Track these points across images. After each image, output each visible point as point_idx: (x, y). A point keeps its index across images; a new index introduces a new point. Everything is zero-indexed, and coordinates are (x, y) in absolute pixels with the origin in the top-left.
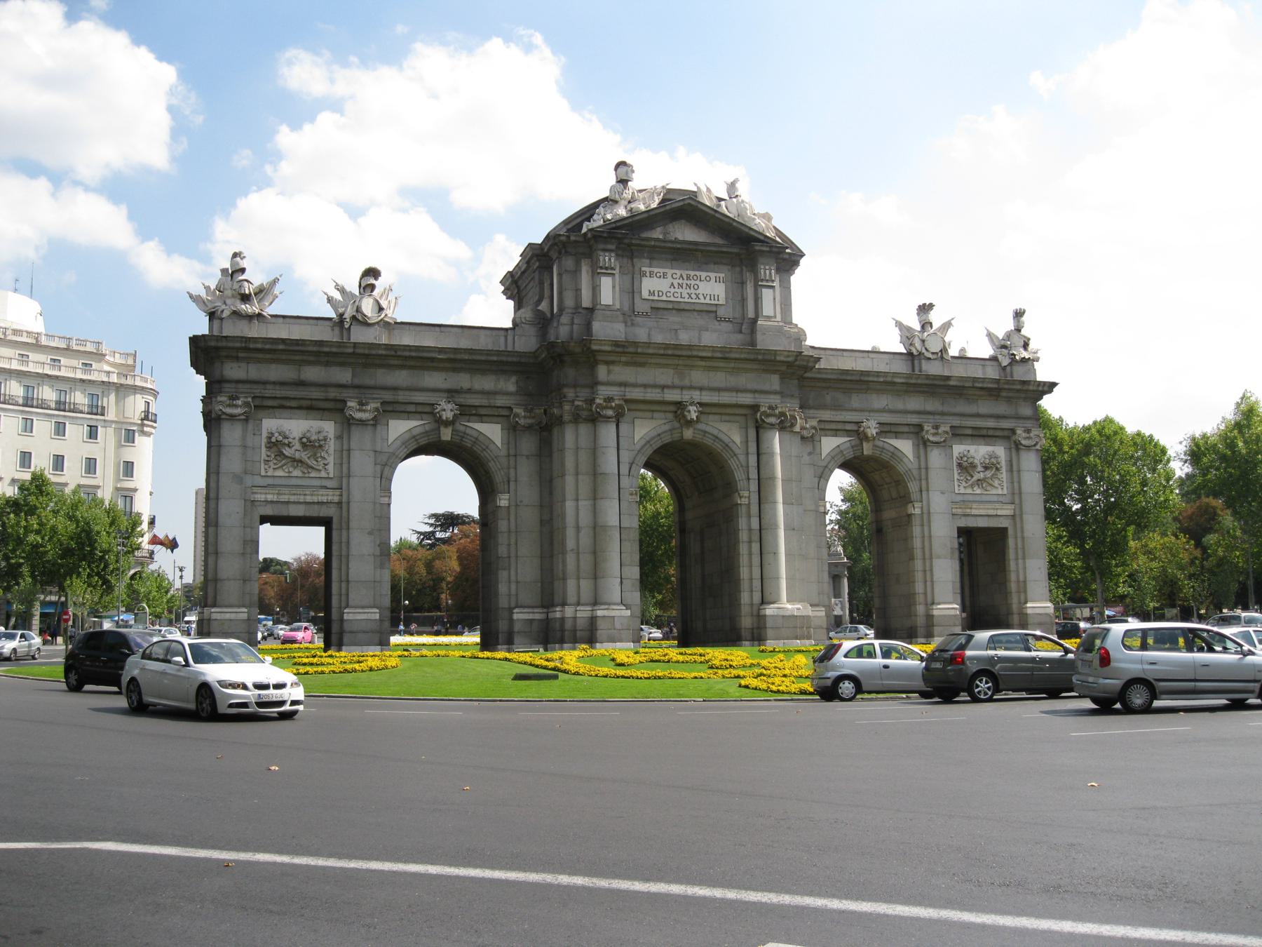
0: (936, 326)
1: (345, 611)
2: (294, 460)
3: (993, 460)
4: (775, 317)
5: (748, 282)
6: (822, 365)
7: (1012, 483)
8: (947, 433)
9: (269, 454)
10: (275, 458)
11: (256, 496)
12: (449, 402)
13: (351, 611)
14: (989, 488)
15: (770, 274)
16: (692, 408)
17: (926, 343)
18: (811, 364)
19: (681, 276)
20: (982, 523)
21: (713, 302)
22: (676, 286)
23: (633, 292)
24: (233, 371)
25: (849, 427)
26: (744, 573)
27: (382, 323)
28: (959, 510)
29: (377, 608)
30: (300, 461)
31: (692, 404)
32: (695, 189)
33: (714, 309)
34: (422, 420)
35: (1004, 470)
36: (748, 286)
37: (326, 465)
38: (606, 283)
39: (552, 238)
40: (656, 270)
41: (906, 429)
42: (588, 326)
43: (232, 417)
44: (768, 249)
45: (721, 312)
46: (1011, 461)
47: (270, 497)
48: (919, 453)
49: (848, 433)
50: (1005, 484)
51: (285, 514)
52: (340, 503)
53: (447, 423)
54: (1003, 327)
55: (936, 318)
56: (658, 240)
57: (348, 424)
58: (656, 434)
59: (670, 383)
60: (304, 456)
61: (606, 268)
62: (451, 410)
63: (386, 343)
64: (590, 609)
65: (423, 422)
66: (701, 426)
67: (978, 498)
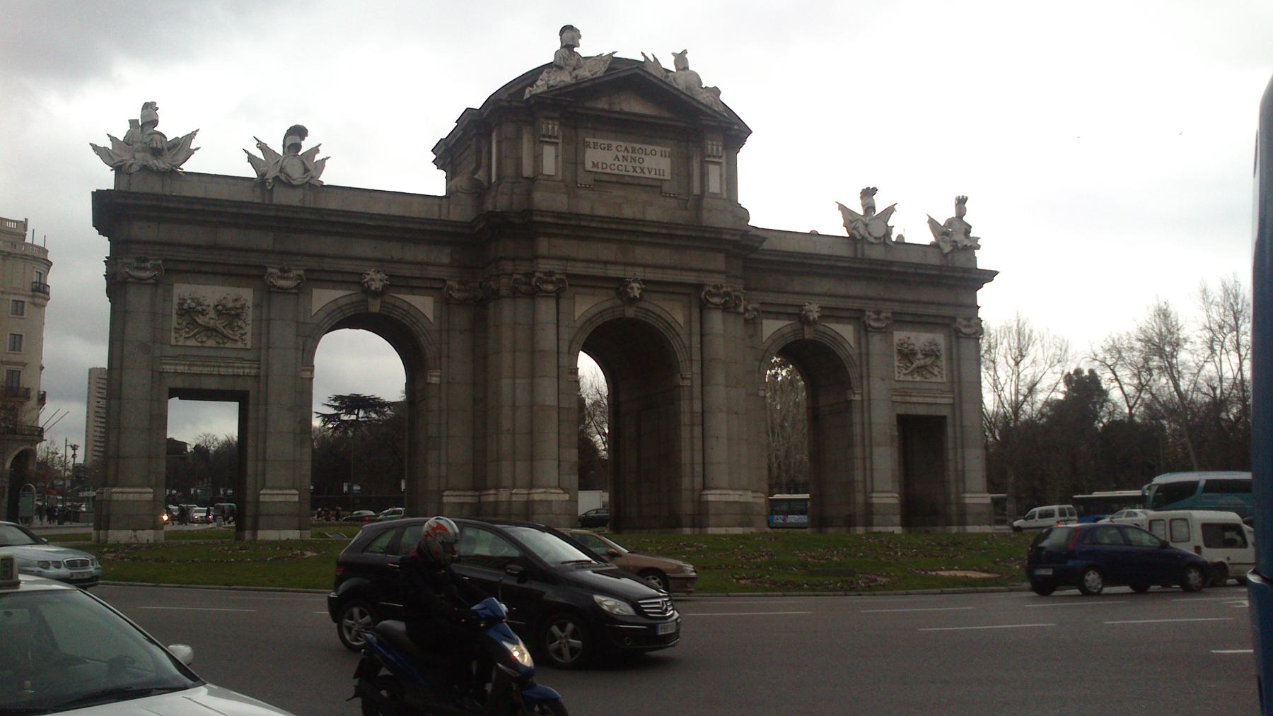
0: (878, 210)
1: (262, 492)
2: (208, 329)
3: (933, 347)
4: (721, 193)
5: (694, 159)
6: (765, 246)
7: (952, 371)
8: (887, 318)
9: (180, 322)
10: (186, 327)
11: (164, 367)
12: (378, 272)
13: (269, 492)
14: (928, 376)
15: (717, 149)
17: (869, 227)
18: (757, 245)
19: (626, 149)
20: (922, 411)
21: (657, 177)
22: (621, 159)
23: (576, 163)
24: (142, 231)
25: (790, 310)
26: (686, 457)
27: (307, 185)
28: (899, 398)
29: (297, 490)
30: (215, 330)
31: (635, 280)
32: (642, 59)
33: (659, 184)
34: (350, 290)
35: (943, 358)
36: (695, 164)
37: (242, 335)
38: (549, 153)
39: (493, 102)
40: (600, 141)
41: (847, 314)
42: (529, 194)
43: (140, 281)
44: (716, 124)
45: (666, 187)
47: (180, 369)
48: (860, 338)
49: (789, 316)
50: (944, 372)
51: (196, 386)
52: (257, 376)
53: (377, 294)
54: (945, 214)
55: (880, 204)
56: (603, 110)
57: (268, 292)
59: (613, 259)
60: (219, 324)
61: (550, 137)
62: (381, 280)
63: (312, 206)
64: (526, 492)
65: (349, 292)
66: (643, 305)
67: (917, 386)
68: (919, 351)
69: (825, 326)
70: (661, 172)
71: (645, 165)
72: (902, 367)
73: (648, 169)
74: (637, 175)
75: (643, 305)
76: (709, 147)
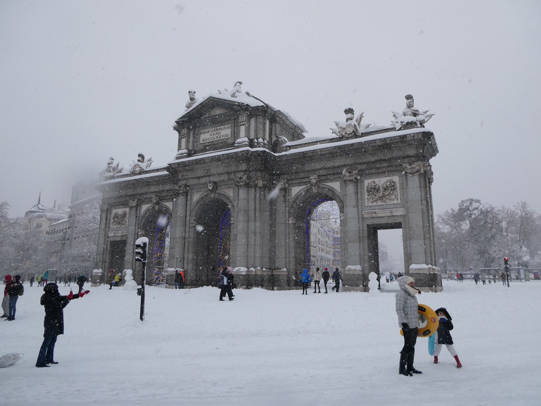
28: (368, 215)
40: (205, 130)
46: (403, 183)
50: (399, 197)
57: (131, 208)
61: (184, 135)
65: (151, 204)
66: (217, 192)
68: (381, 188)
70: (227, 135)
71: (221, 134)
72: (370, 199)
74: (218, 139)
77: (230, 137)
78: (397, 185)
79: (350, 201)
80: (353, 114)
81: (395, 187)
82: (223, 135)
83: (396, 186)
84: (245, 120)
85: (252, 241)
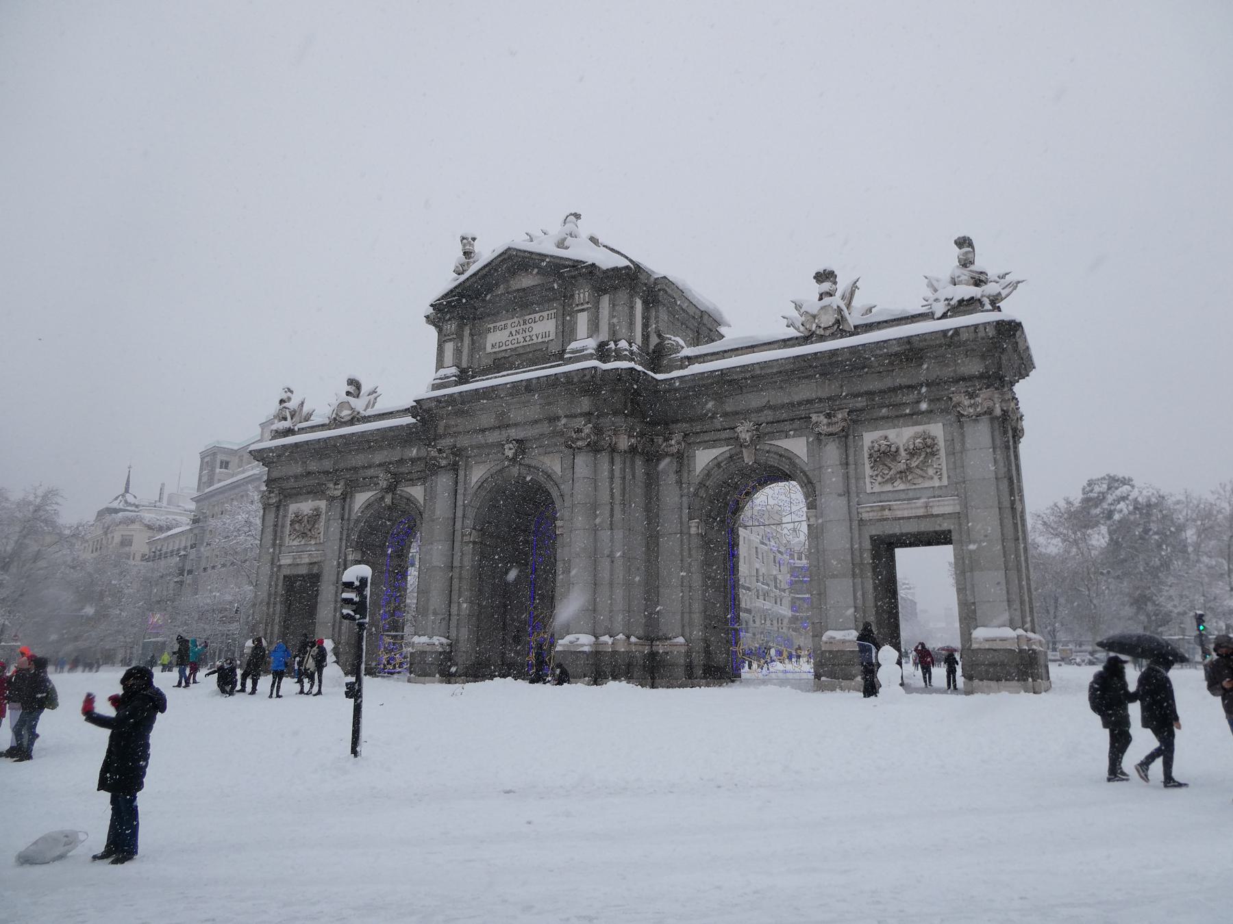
14: (920, 480)
16: (506, 446)
21: (543, 340)
28: (871, 514)
31: (508, 441)
35: (942, 453)
37: (319, 534)
40: (498, 324)
49: (728, 441)
57: (332, 499)
58: (488, 475)
67: (903, 496)
69: (771, 444)
70: (547, 334)
71: (534, 333)
72: (877, 476)
73: (536, 335)
75: (527, 461)
76: (577, 297)
77: (554, 338)
78: (940, 444)
79: (832, 478)
80: (835, 283)
81: (935, 449)
82: (538, 333)
83: (936, 446)
84: (587, 300)
85: (605, 575)
